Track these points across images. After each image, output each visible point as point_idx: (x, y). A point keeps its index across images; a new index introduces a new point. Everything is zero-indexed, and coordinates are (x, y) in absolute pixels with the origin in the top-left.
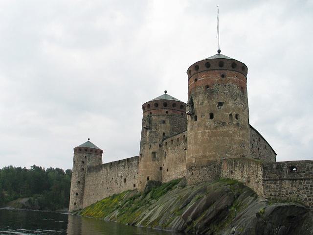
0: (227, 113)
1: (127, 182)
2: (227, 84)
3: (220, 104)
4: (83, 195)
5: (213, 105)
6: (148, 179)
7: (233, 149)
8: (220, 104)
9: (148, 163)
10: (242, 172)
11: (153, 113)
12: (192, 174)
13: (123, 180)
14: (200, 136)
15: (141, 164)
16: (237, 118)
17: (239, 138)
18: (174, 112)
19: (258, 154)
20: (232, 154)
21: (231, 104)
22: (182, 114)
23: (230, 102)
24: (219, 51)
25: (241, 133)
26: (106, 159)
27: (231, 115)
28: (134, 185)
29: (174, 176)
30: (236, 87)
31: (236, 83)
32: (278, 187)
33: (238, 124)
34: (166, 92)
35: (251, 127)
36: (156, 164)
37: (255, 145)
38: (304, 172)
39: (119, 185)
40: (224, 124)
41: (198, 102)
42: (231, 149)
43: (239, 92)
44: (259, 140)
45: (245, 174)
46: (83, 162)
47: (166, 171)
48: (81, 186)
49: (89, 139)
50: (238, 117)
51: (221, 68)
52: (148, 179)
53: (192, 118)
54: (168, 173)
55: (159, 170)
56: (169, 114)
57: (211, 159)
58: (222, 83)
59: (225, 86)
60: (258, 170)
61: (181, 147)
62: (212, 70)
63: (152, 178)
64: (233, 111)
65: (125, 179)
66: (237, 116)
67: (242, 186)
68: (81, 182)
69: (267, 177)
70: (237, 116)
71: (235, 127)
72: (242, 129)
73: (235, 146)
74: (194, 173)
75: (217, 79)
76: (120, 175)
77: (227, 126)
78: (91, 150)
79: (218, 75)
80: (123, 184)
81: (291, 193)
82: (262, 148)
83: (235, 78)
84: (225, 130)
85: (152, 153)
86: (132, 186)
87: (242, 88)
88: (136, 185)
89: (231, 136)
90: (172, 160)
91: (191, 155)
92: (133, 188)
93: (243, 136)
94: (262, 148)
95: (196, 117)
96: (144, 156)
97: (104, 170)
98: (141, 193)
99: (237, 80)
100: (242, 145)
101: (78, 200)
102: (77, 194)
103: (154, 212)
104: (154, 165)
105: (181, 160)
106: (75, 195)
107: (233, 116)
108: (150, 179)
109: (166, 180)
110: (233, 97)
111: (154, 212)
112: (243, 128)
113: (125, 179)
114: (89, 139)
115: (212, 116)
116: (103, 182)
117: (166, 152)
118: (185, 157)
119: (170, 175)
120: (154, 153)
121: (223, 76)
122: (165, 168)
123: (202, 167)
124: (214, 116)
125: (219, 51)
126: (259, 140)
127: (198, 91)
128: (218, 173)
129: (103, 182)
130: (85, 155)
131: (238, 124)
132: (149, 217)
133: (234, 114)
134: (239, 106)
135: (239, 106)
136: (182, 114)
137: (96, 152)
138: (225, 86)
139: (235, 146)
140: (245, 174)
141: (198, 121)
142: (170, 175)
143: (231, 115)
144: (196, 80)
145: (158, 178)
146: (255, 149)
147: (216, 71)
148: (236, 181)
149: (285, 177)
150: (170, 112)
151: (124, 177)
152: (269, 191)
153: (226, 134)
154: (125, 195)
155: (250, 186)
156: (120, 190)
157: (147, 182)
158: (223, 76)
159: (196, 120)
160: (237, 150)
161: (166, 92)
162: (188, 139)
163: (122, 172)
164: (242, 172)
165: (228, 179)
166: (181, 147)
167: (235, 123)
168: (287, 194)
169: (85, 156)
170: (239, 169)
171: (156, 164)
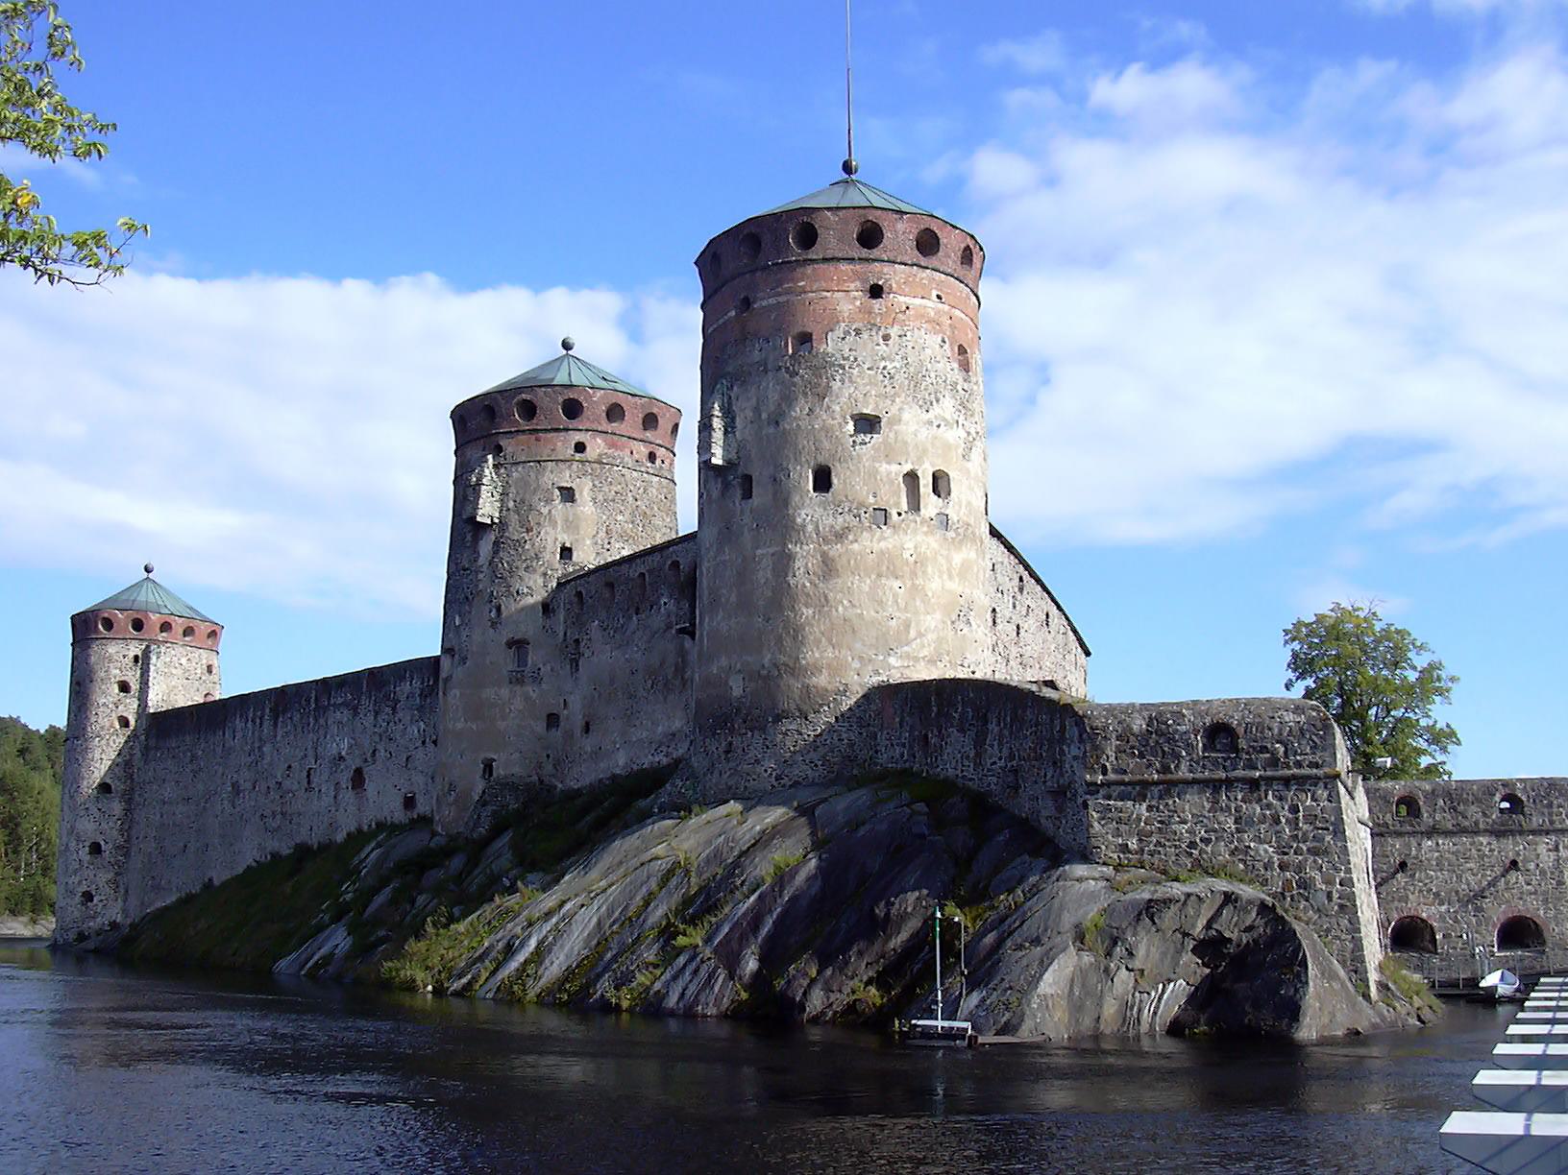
0: (894, 468)
1: (370, 787)
2: (894, 332)
3: (867, 424)
4: (127, 855)
5: (827, 430)
6: (488, 766)
7: (920, 635)
8: (867, 424)
9: (489, 693)
10: (979, 743)
11: (510, 449)
12: (727, 752)
13: (345, 778)
14: (764, 574)
15: (453, 698)
16: (936, 491)
18: (612, 445)
19: (1014, 651)
20: (916, 659)
22: (652, 457)
23: (906, 416)
28: (409, 802)
29: (621, 759)
30: (931, 349)
31: (935, 323)
32: (1154, 814)
34: (567, 346)
35: (994, 533)
36: (527, 698)
37: (1005, 611)
38: (1264, 749)
39: (327, 800)
40: (883, 516)
41: (757, 410)
42: (913, 634)
43: (951, 370)
44: (1021, 590)
45: (995, 756)
46: (124, 687)
47: (578, 732)
48: (117, 807)
50: (941, 484)
51: (865, 253)
52: (488, 766)
53: (726, 486)
54: (588, 744)
55: (540, 727)
56: (591, 453)
57: (822, 680)
59: (886, 338)
60: (1062, 740)
61: (657, 621)
62: (825, 260)
63: (510, 765)
64: (920, 460)
65: (359, 772)
66: (937, 477)
67: (982, 809)
68: (117, 786)
69: (1105, 773)
71: (930, 532)
74: (736, 741)
75: (847, 301)
76: (333, 749)
79: (852, 286)
80: (348, 796)
81: (1206, 841)
82: (1030, 624)
83: (932, 304)
84: (883, 544)
85: (510, 644)
86: (398, 803)
87: (962, 350)
88: (420, 799)
89: (914, 574)
90: (612, 681)
91: (724, 662)
92: (400, 816)
94: (1030, 624)
95: (748, 479)
96: (464, 660)
97: (239, 723)
98: (452, 838)
99: (938, 312)
100: (961, 615)
101: (104, 877)
102: (96, 849)
103: (558, 932)
104: (518, 704)
105: (670, 679)
106: (84, 853)
107: (922, 482)
108: (499, 771)
109: (583, 776)
111: (558, 932)
112: (966, 536)
113: (359, 772)
114: (148, 570)
115: (823, 480)
116: (235, 785)
117: (577, 641)
118: (680, 669)
119: (597, 754)
120: (518, 645)
122: (574, 714)
123: (778, 719)
124: (835, 480)
125: (847, 168)
126: (1021, 590)
127: (756, 356)
128: (851, 745)
129: (235, 785)
130: (136, 649)
131: (945, 521)
132: (540, 955)
136: (652, 457)
137: (188, 631)
138: (886, 338)
140: (995, 756)
141: (758, 498)
142: (597, 754)
143: (912, 478)
144: (747, 303)
145: (540, 765)
146: (1006, 629)
147: (844, 267)
148: (949, 786)
149: (1183, 772)
150: (596, 446)
151: (354, 763)
152: (1118, 834)
153: (889, 566)
154: (371, 854)
155: (1023, 806)
156: (333, 826)
157: (480, 786)
158: (876, 292)
159: (748, 494)
160: (940, 640)
161: (567, 346)
162: (704, 583)
164: (979, 743)
165: (904, 771)
166: (657, 621)
168: (1192, 845)
169: (132, 655)
170: (962, 730)
171: (527, 698)
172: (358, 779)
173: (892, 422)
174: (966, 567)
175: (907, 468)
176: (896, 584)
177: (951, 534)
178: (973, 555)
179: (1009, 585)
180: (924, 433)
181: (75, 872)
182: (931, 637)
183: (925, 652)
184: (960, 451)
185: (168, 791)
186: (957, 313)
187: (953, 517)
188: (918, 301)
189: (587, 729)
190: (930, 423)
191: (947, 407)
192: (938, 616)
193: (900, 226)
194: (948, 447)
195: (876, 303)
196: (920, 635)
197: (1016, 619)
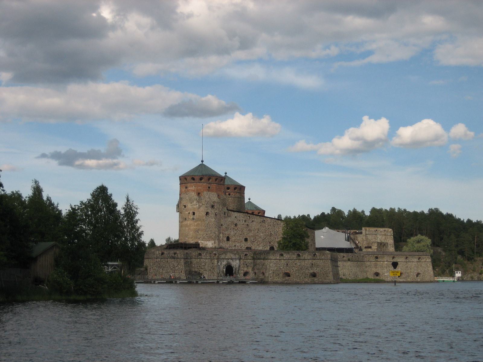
0: (187, 212)
2: (188, 193)
17: (194, 227)
20: (189, 238)
21: (189, 206)
22: (229, 194)
23: (189, 205)
24: (202, 161)
25: (196, 224)
27: (189, 213)
30: (194, 195)
31: (194, 191)
33: (193, 219)
43: (196, 197)
49: (249, 199)
58: (186, 193)
59: (187, 194)
70: (194, 214)
71: (191, 221)
72: (196, 222)
73: (191, 233)
77: (187, 221)
79: (184, 187)
93: (197, 225)
99: (194, 189)
110: (191, 201)
121: (186, 187)
125: (202, 161)
133: (191, 212)
134: (195, 207)
135: (195, 207)
138: (187, 194)
139: (191, 233)
147: (183, 184)
167: (192, 218)
173: (187, 206)
174: (198, 224)
175: (189, 212)
176: (187, 228)
177: (195, 220)
178: (200, 222)
179: (242, 219)
180: (191, 207)
182: (191, 235)
183: (190, 237)
184: (197, 209)
186: (199, 188)
187: (195, 218)
188: (191, 188)
190: (192, 206)
191: (195, 202)
192: (192, 232)
193: (189, 178)
194: (194, 208)
195: (186, 190)
196: (190, 235)
197: (247, 223)
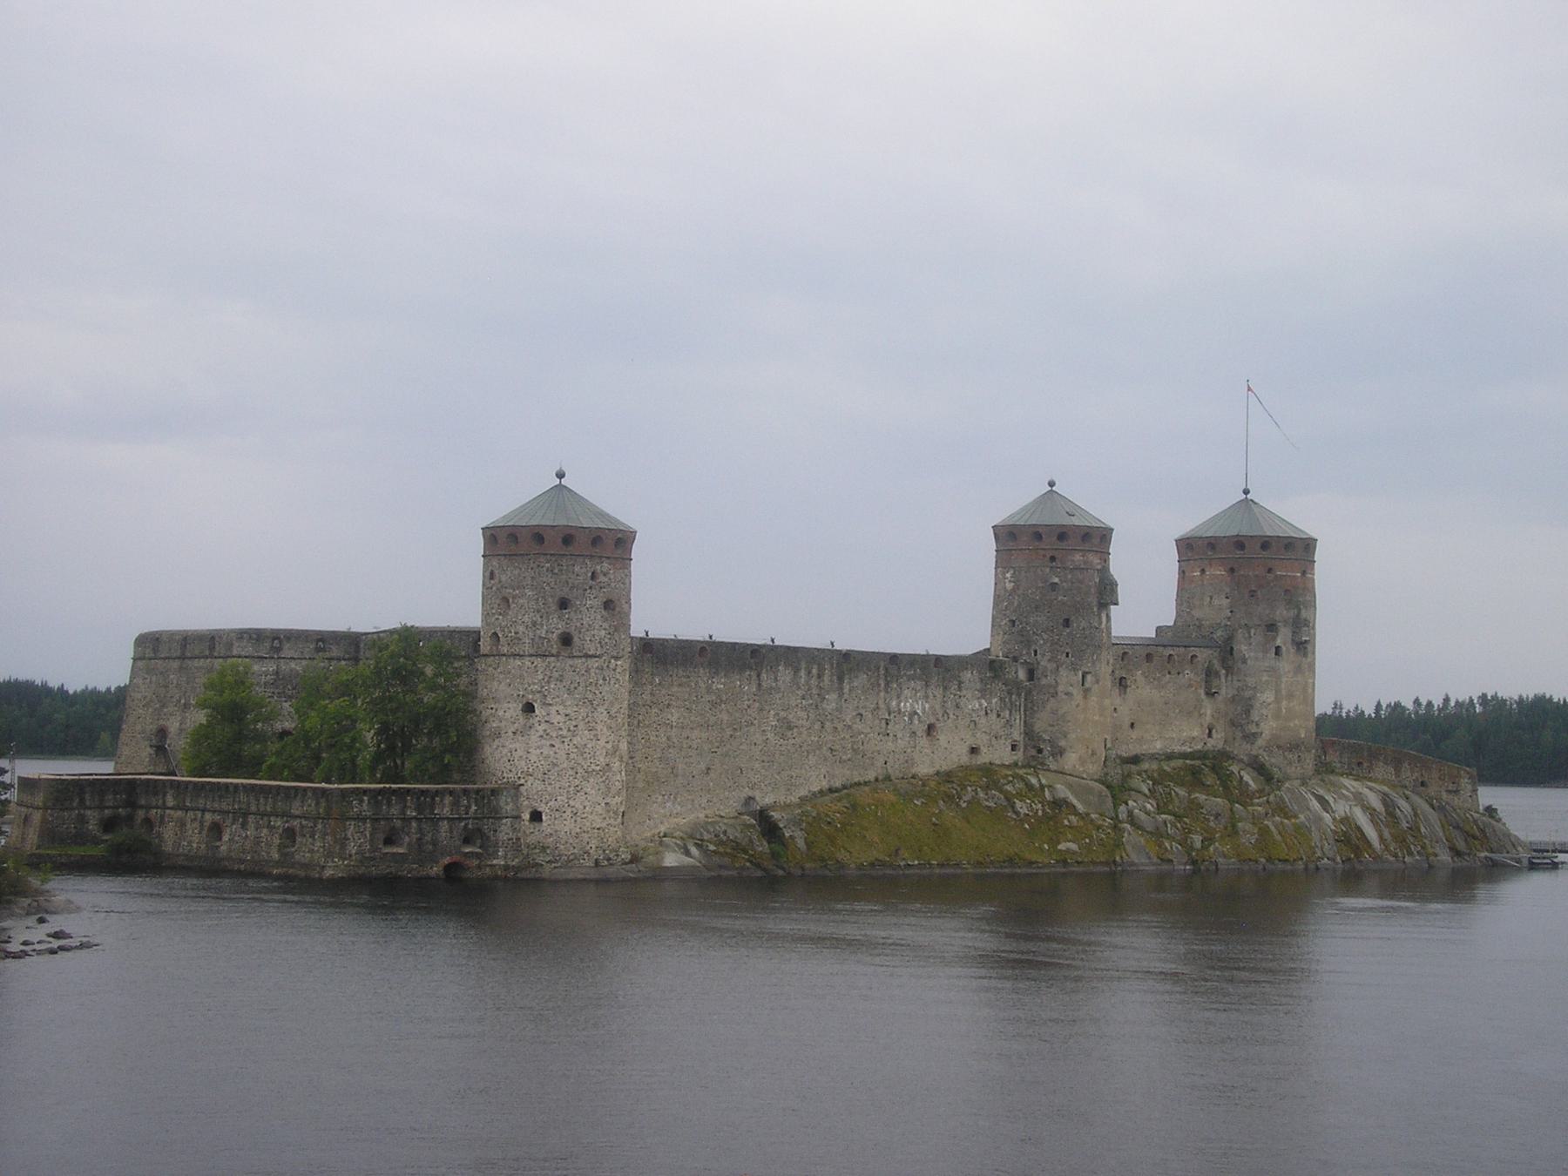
1: (942, 737)
13: (921, 729)
24: (1246, 492)
26: (663, 603)
28: (974, 750)
34: (1051, 484)
49: (561, 475)
54: (1134, 734)
76: (906, 706)
78: (568, 538)
80: (923, 741)
86: (965, 750)
88: (984, 750)
92: (965, 759)
114: (561, 475)
119: (1140, 740)
156: (909, 762)
161: (1051, 484)
163: (914, 702)
172: (930, 729)
181: (618, 794)
185: (674, 716)
189: (1132, 725)
